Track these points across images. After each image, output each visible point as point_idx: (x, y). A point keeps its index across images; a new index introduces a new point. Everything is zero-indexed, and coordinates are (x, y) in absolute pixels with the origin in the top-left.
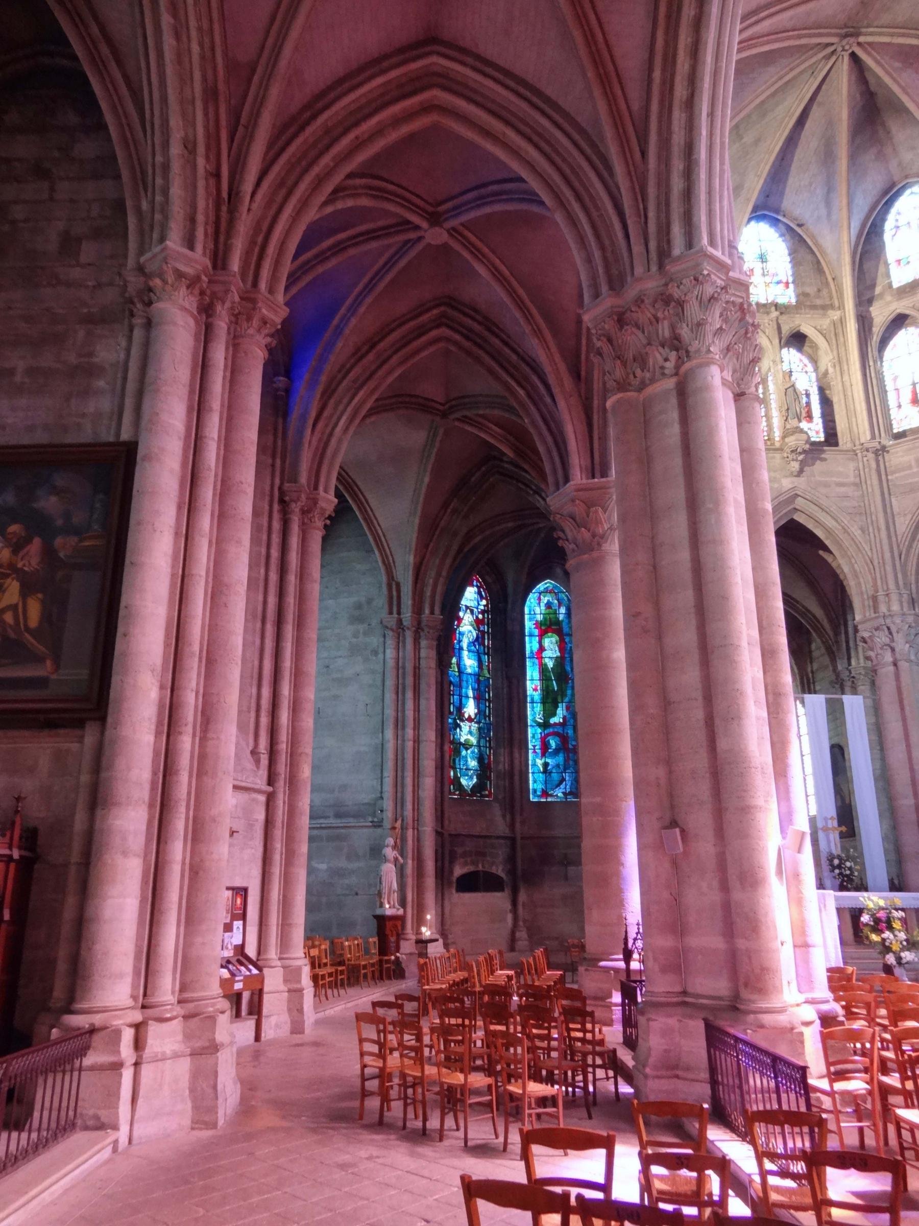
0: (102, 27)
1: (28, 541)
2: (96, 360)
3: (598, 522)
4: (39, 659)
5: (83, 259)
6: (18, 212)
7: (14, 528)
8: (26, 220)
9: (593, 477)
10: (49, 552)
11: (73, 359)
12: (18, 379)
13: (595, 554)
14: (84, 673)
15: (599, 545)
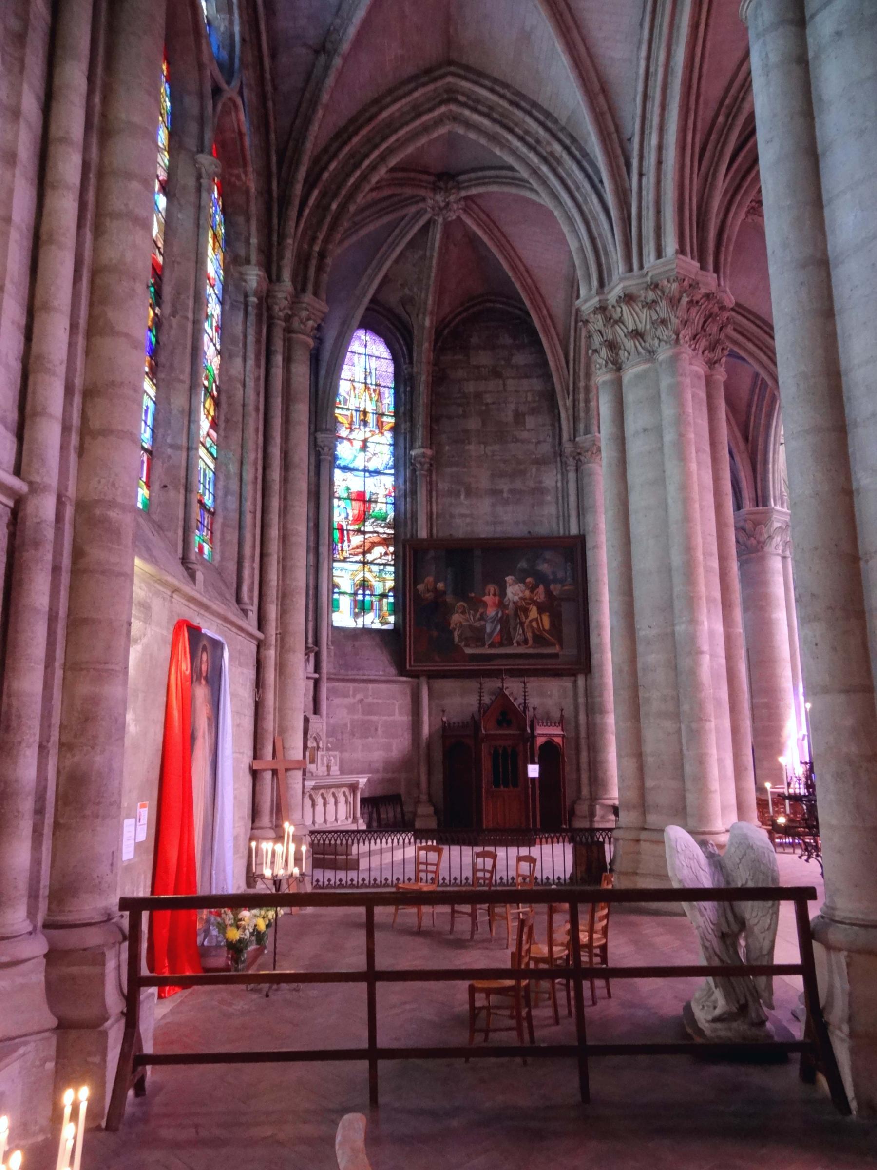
0: (548, 310)
1: (537, 587)
2: (544, 485)
3: (761, 534)
4: (553, 645)
5: (528, 426)
6: (488, 399)
7: (528, 580)
8: (493, 403)
9: (757, 506)
10: (548, 593)
11: (531, 484)
12: (505, 495)
13: (760, 554)
14: (574, 652)
15: (762, 548)
